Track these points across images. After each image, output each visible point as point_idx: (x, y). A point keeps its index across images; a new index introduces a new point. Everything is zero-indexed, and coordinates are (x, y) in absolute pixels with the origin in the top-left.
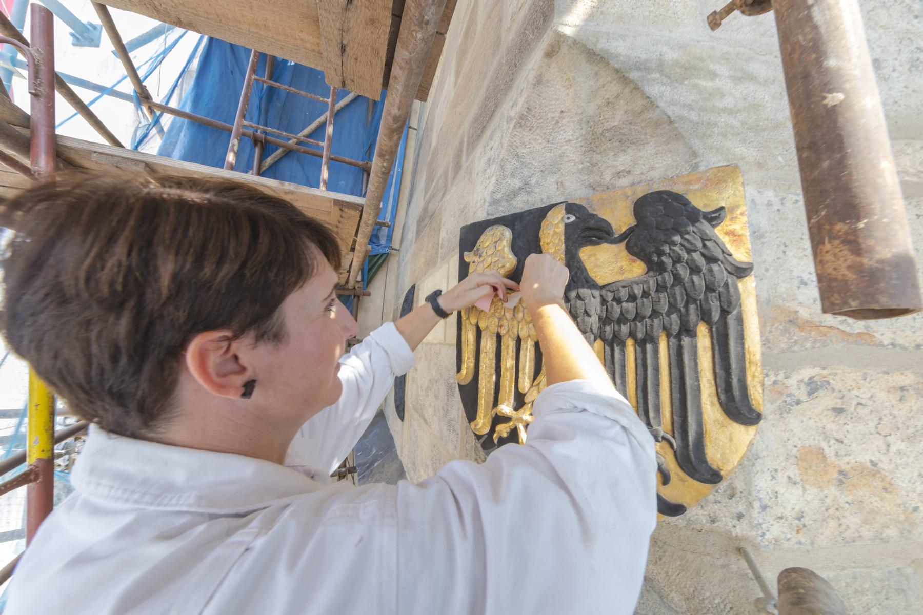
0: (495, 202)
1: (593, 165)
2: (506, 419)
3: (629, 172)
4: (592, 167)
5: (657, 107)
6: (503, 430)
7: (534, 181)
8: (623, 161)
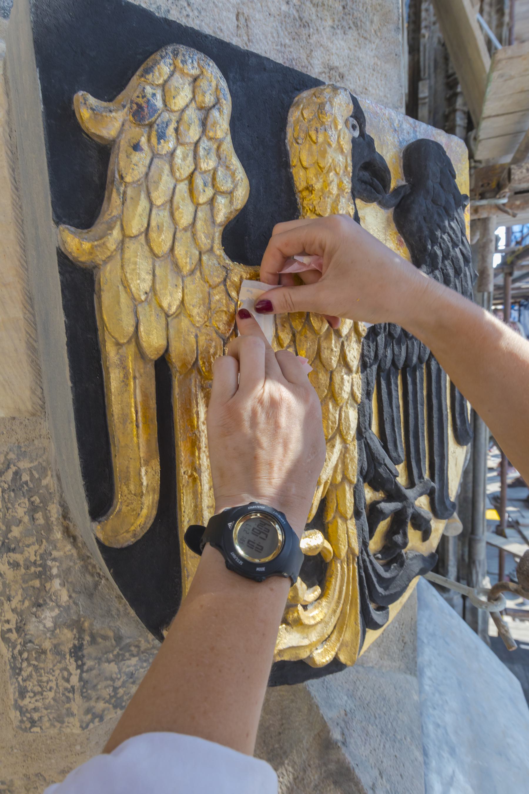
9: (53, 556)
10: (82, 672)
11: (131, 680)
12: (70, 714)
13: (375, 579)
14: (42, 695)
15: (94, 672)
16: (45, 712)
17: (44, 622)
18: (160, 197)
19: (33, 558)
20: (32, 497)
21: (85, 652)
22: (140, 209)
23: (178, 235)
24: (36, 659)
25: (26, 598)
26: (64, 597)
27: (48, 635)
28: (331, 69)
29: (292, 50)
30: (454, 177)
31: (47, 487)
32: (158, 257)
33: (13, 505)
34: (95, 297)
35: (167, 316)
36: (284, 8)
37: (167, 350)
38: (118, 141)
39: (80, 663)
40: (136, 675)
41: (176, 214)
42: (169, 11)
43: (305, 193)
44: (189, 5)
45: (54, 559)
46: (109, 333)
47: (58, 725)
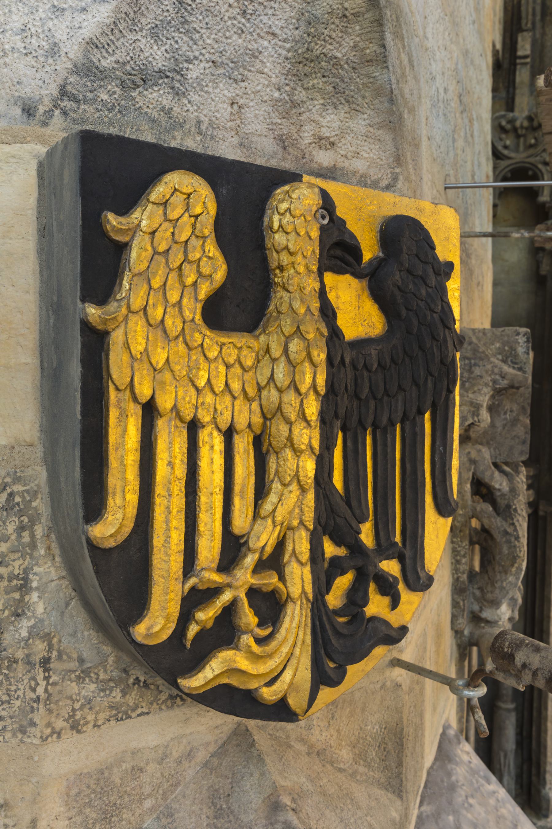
0: (87, 70)
1: (295, 105)
2: (214, 592)
3: (333, 144)
4: (290, 108)
5: (387, 67)
6: (206, 615)
7: (194, 72)
8: (331, 122)
9: (34, 571)
10: (48, 684)
11: (88, 706)
12: (33, 724)
13: (330, 632)
14: (9, 703)
15: (58, 688)
16: (9, 721)
17: (20, 631)
18: (156, 283)
19: (16, 572)
20: (22, 516)
21: (52, 666)
22: (142, 293)
23: (168, 310)
24: (8, 668)
25: (7, 607)
26: (40, 609)
27: (22, 644)
28: (321, 139)
29: (283, 127)
30: (433, 248)
31: (36, 509)
32: (150, 325)
33: (4, 523)
34: (103, 354)
35: (155, 370)
36: (276, 94)
37: (153, 397)
38: (130, 244)
39: (47, 674)
40: (93, 703)
41: (168, 294)
42: (172, 109)
43: (278, 271)
44: (189, 102)
45: (35, 574)
46: (113, 382)
47: (20, 736)
